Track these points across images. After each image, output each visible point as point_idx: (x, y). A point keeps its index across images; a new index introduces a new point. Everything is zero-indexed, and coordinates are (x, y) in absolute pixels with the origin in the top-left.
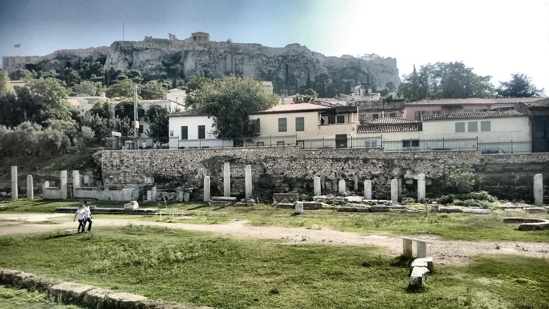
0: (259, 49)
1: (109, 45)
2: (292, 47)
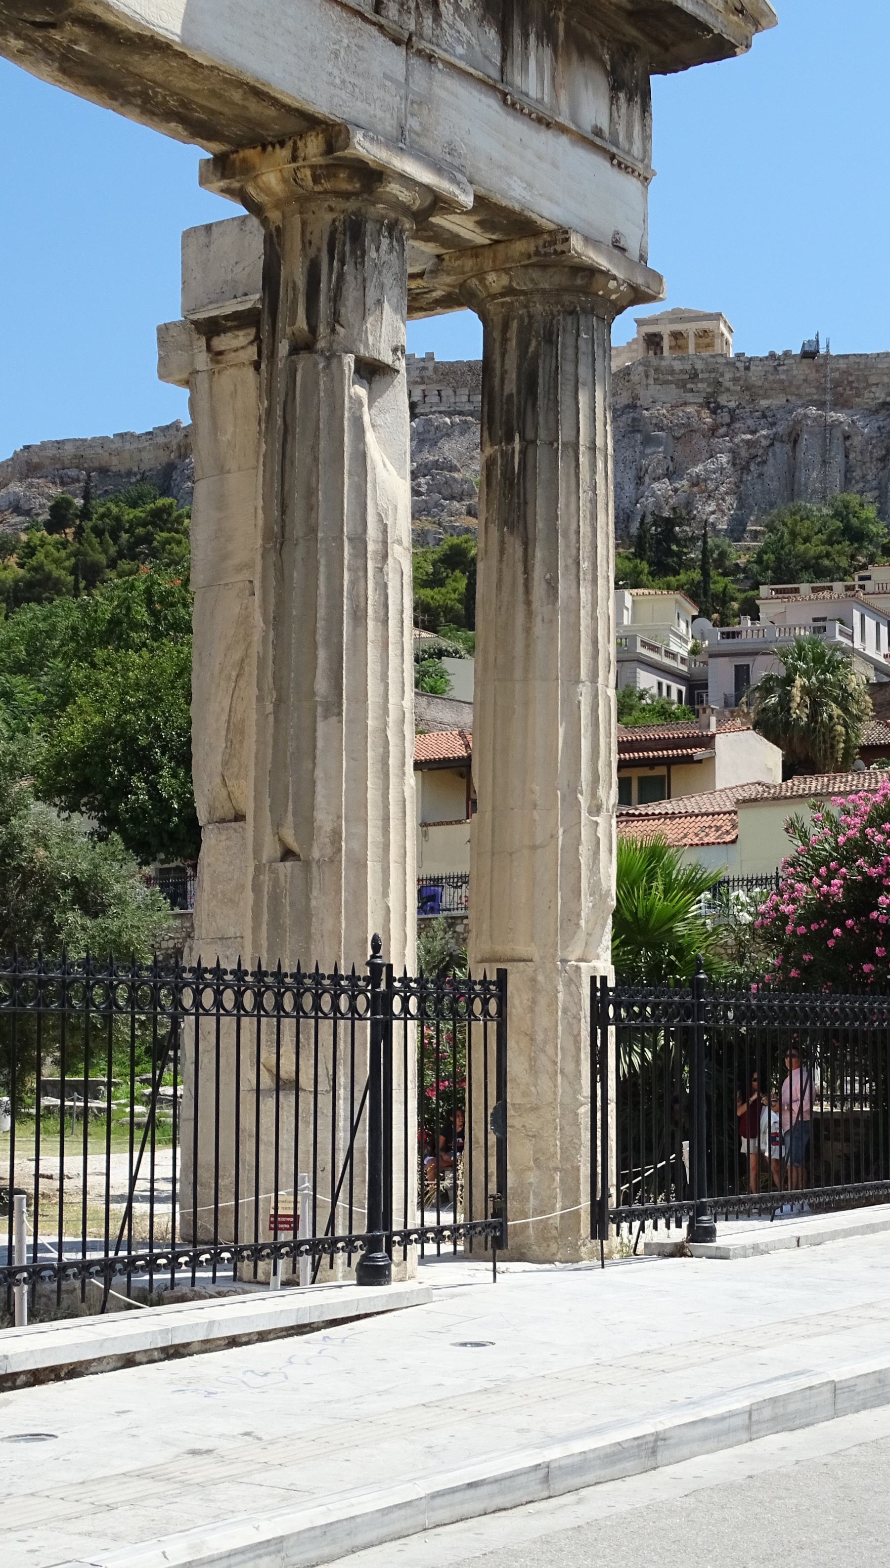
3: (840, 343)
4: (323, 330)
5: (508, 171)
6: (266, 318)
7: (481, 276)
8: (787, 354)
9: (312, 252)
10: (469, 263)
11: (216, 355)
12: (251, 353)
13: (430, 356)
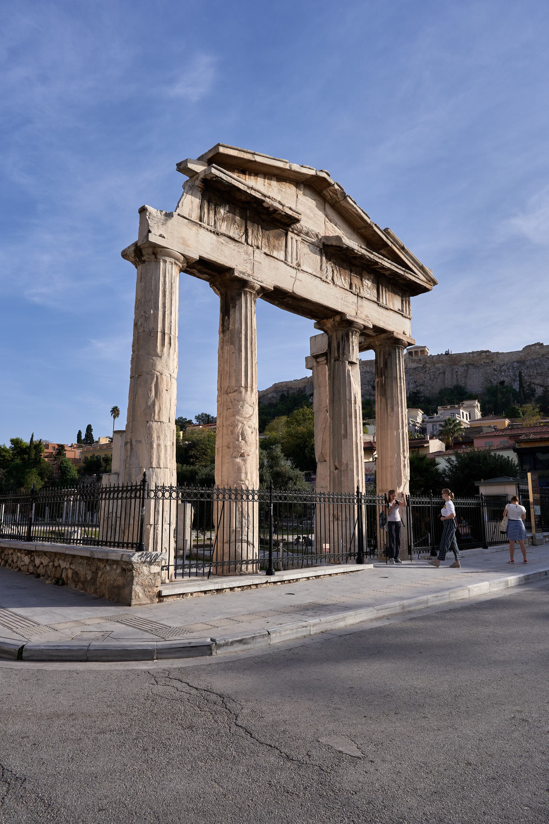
0: (487, 356)
2: (533, 348)
3: (454, 352)
4: (341, 356)
5: (379, 320)
6: (329, 354)
7: (374, 342)
8: (442, 354)
9: (338, 340)
10: (371, 340)
11: (318, 363)
12: (325, 361)
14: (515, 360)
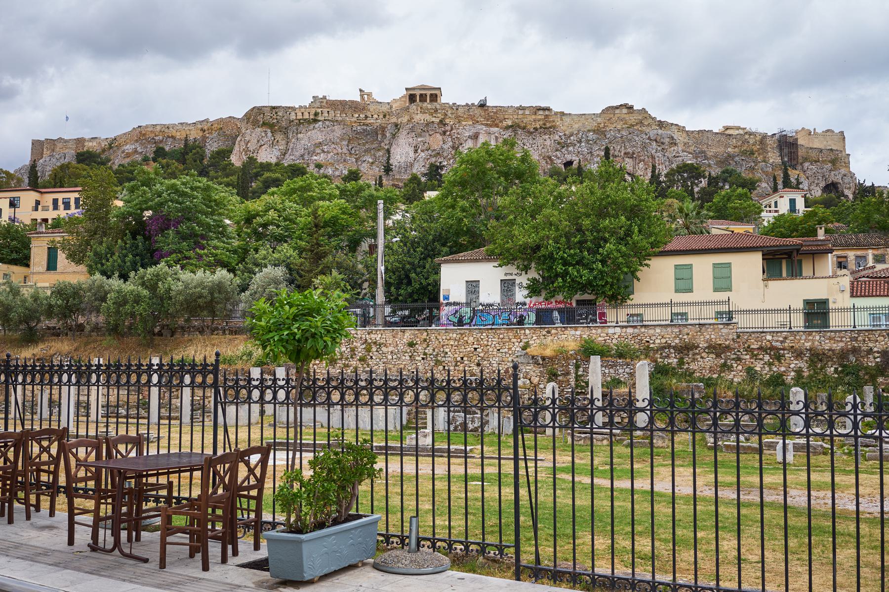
1: (239, 113)
2: (617, 111)
8: (473, 104)
13: (325, 97)
14: (589, 128)
